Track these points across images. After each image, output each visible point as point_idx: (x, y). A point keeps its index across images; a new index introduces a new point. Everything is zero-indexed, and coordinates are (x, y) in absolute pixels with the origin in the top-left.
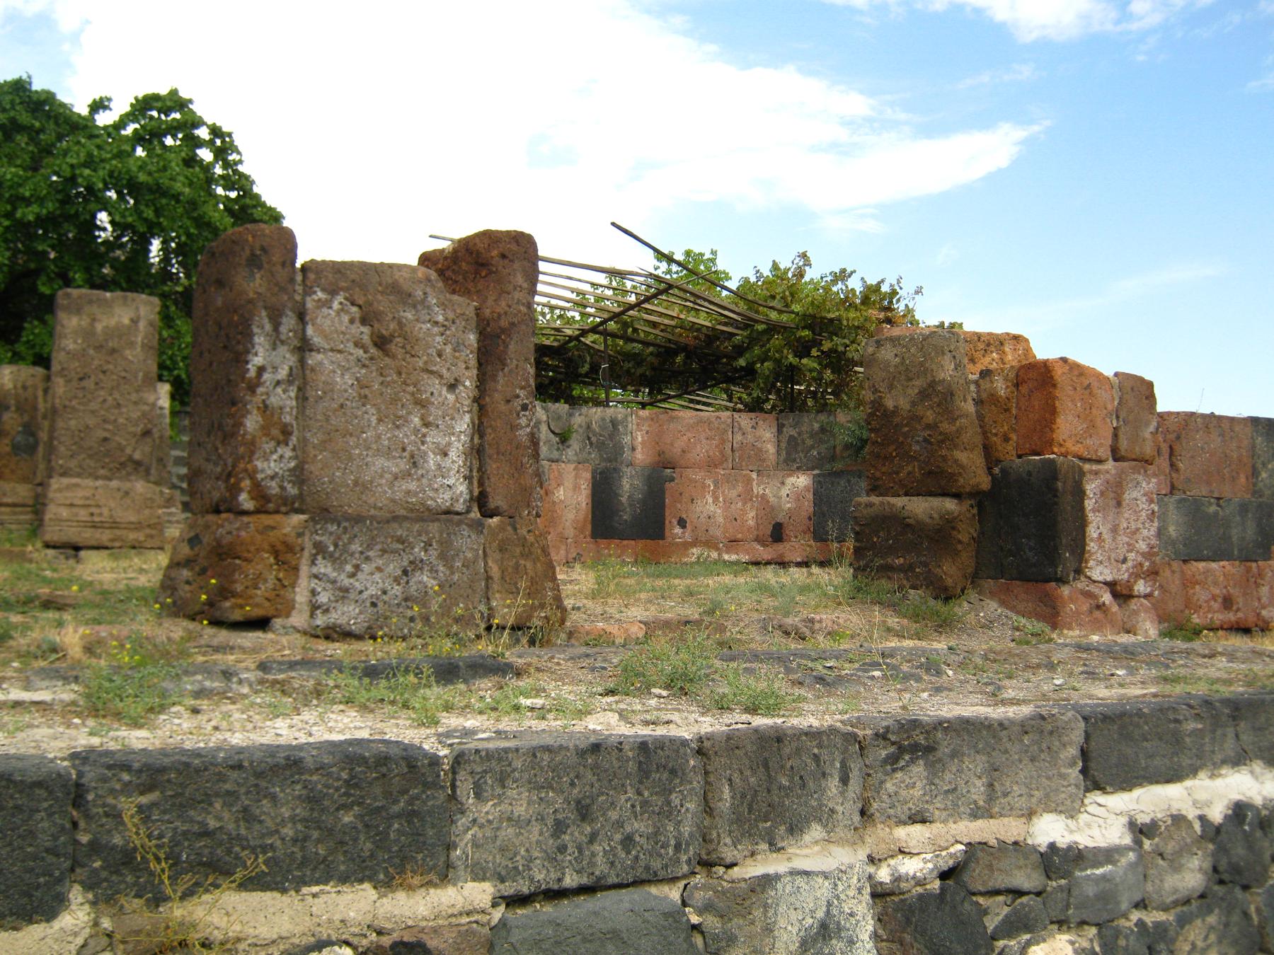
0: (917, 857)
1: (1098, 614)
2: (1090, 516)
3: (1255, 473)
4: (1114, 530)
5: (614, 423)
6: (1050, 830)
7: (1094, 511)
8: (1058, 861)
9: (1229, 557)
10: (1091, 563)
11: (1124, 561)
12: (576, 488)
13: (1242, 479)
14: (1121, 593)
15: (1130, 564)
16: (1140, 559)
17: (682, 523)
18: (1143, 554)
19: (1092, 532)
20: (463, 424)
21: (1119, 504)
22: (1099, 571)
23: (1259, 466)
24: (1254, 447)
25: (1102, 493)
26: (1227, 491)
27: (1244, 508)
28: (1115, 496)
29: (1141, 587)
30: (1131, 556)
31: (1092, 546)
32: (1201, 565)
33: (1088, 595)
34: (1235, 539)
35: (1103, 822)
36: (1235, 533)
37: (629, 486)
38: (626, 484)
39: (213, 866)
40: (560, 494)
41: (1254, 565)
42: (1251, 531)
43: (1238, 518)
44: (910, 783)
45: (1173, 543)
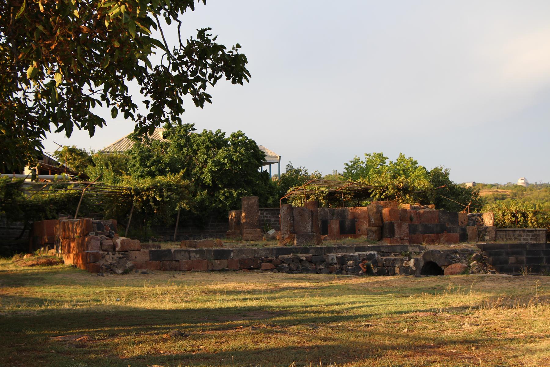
0: (340, 255)
5: (344, 211)
6: (351, 254)
8: (352, 256)
12: (336, 225)
14: (402, 239)
17: (359, 230)
19: (396, 231)
20: (310, 223)
22: (397, 236)
28: (400, 226)
29: (405, 238)
35: (357, 254)
37: (347, 223)
38: (347, 223)
39: (297, 252)
40: (333, 226)
44: (340, 250)
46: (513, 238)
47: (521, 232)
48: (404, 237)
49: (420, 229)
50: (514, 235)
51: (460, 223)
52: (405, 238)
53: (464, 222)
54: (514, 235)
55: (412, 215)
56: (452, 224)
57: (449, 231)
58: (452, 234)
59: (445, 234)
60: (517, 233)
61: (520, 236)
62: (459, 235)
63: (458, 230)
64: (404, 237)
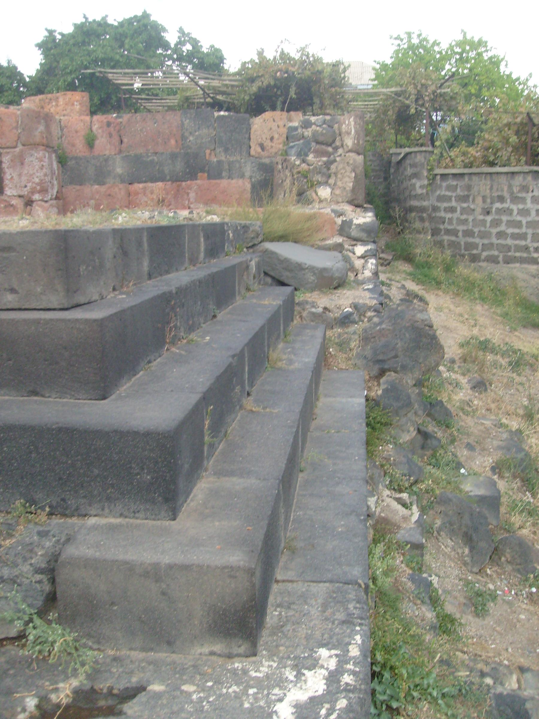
1: (12, 209)
2: (7, 170)
3: (184, 138)
4: (20, 175)
7: (8, 168)
9: (162, 179)
10: (7, 189)
11: (26, 186)
13: (173, 142)
15: (28, 188)
16: (34, 185)
18: (37, 184)
19: (8, 176)
21: (22, 164)
23: (187, 134)
24: (183, 124)
25: (12, 161)
26: (160, 149)
27: (174, 156)
28: (20, 160)
29: (36, 197)
30: (29, 185)
31: (6, 182)
32: (141, 186)
33: (6, 201)
34: (167, 172)
36: (166, 170)
41: (184, 183)
42: (179, 166)
43: (170, 162)
45: (120, 176)
46: (506, 195)
47: (529, 178)
48: (33, 192)
49: (119, 170)
50: (510, 186)
51: (255, 150)
52: (36, 197)
53: (268, 143)
54: (510, 186)
55: (95, 128)
56: (226, 150)
57: (215, 173)
58: (224, 183)
59: (201, 181)
60: (518, 180)
61: (525, 188)
62: (248, 186)
63: (248, 170)
64: (33, 192)
